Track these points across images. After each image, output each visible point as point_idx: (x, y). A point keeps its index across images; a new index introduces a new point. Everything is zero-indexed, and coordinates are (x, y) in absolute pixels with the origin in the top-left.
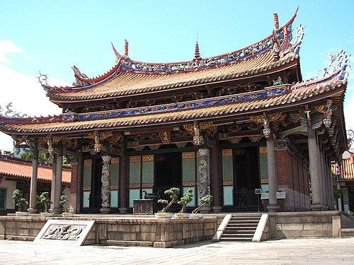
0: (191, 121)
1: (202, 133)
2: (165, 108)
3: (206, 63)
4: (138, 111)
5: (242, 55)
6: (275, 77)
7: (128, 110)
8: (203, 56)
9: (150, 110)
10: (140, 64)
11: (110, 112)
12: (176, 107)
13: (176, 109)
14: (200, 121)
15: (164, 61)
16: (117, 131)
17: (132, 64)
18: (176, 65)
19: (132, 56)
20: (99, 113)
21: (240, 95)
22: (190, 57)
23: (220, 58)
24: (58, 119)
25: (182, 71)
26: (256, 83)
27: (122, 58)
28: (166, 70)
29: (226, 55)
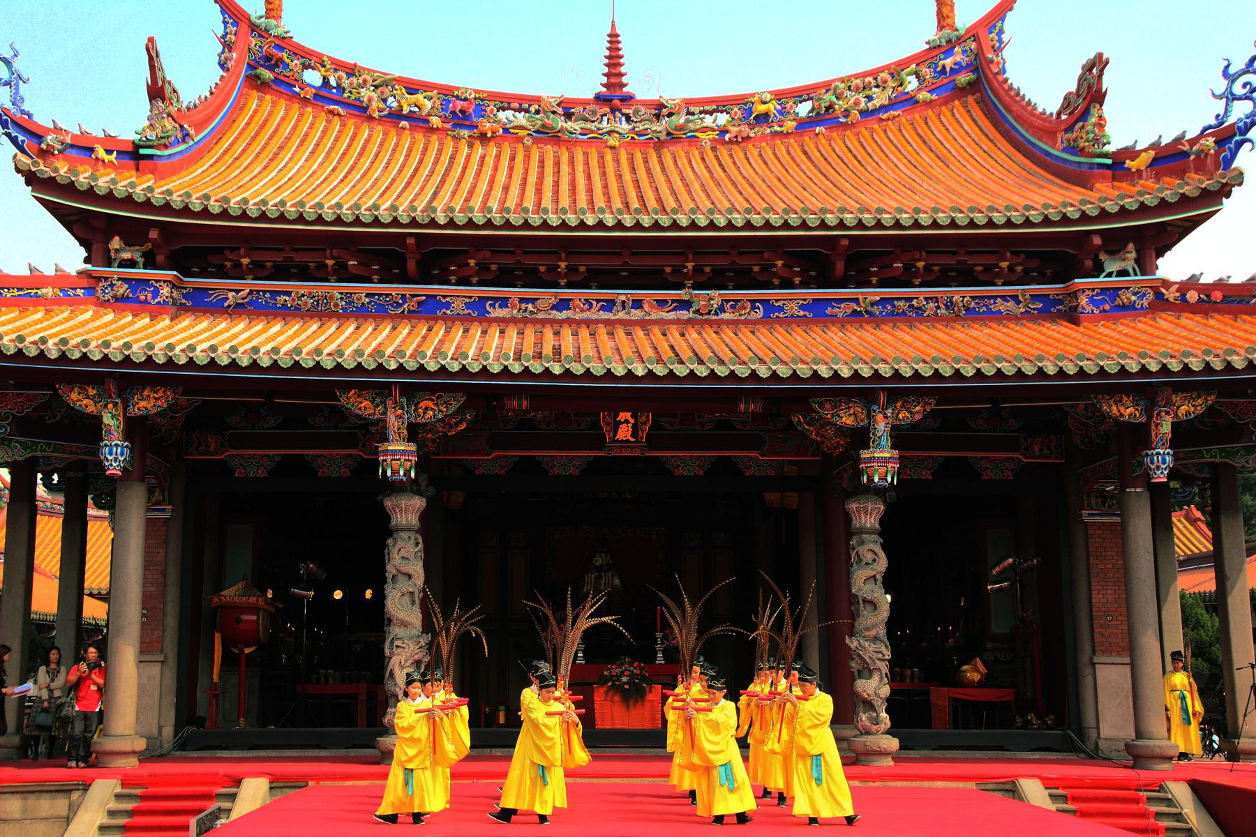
0: (866, 391)
1: (900, 437)
2: (638, 304)
3: (658, 116)
4: (504, 302)
5: (804, 109)
6: (1115, 242)
7: (457, 295)
8: (639, 85)
9: (563, 304)
10: (352, 70)
11: (361, 290)
12: (685, 305)
13: (684, 315)
14: (898, 389)
15: (471, 77)
16: (483, 395)
17: (306, 67)
18: (521, 103)
19: (302, 24)
20: (299, 287)
21: (960, 294)
22: (589, 84)
23: (721, 104)
24: (69, 291)
25: (547, 135)
26: (1030, 255)
27: (254, 27)
28: (463, 114)
29: (742, 101)
